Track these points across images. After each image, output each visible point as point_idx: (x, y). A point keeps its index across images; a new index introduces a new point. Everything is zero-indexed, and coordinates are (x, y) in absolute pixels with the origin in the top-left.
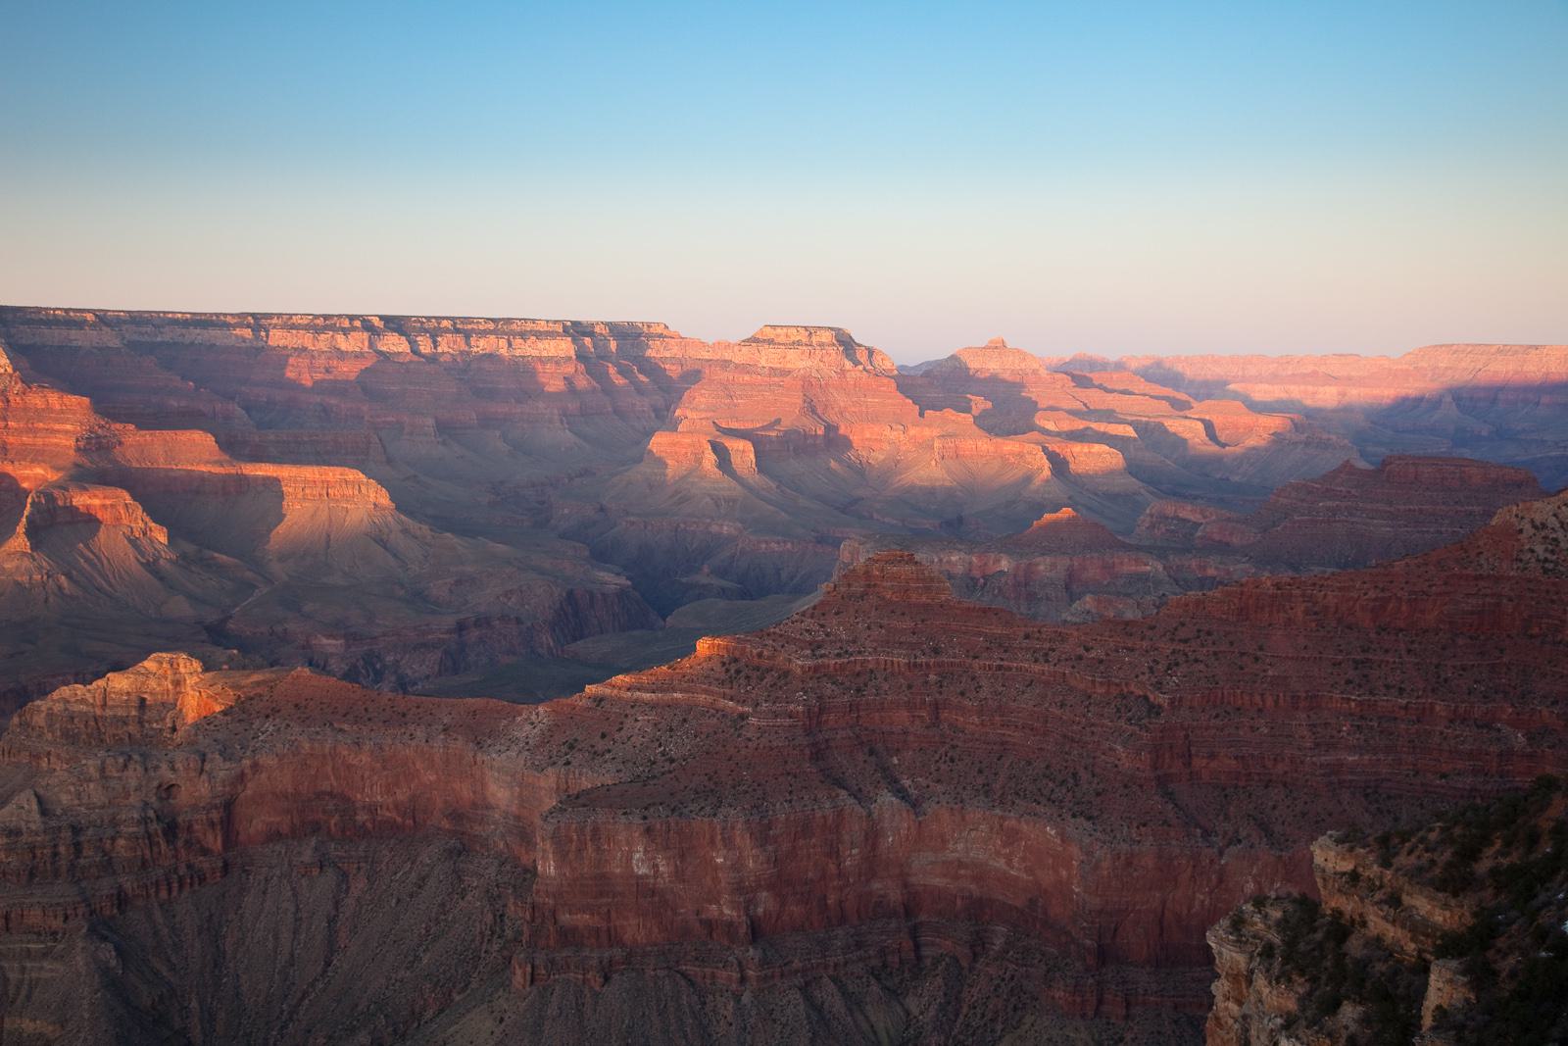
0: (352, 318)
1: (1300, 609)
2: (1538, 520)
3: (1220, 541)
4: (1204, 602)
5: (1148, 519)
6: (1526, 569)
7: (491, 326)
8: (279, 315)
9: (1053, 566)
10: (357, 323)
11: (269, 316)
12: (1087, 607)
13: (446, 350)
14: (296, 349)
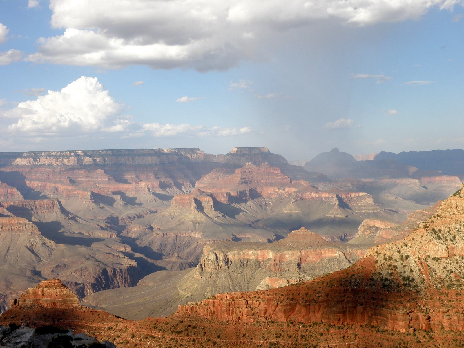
0: (70, 152)
1: (245, 311)
2: (388, 254)
3: (386, 238)
4: (196, 308)
5: (362, 228)
6: (374, 285)
7: (127, 152)
8: (45, 152)
9: (293, 255)
10: (73, 154)
11: (41, 152)
12: (267, 283)
13: (108, 163)
14: (49, 165)
